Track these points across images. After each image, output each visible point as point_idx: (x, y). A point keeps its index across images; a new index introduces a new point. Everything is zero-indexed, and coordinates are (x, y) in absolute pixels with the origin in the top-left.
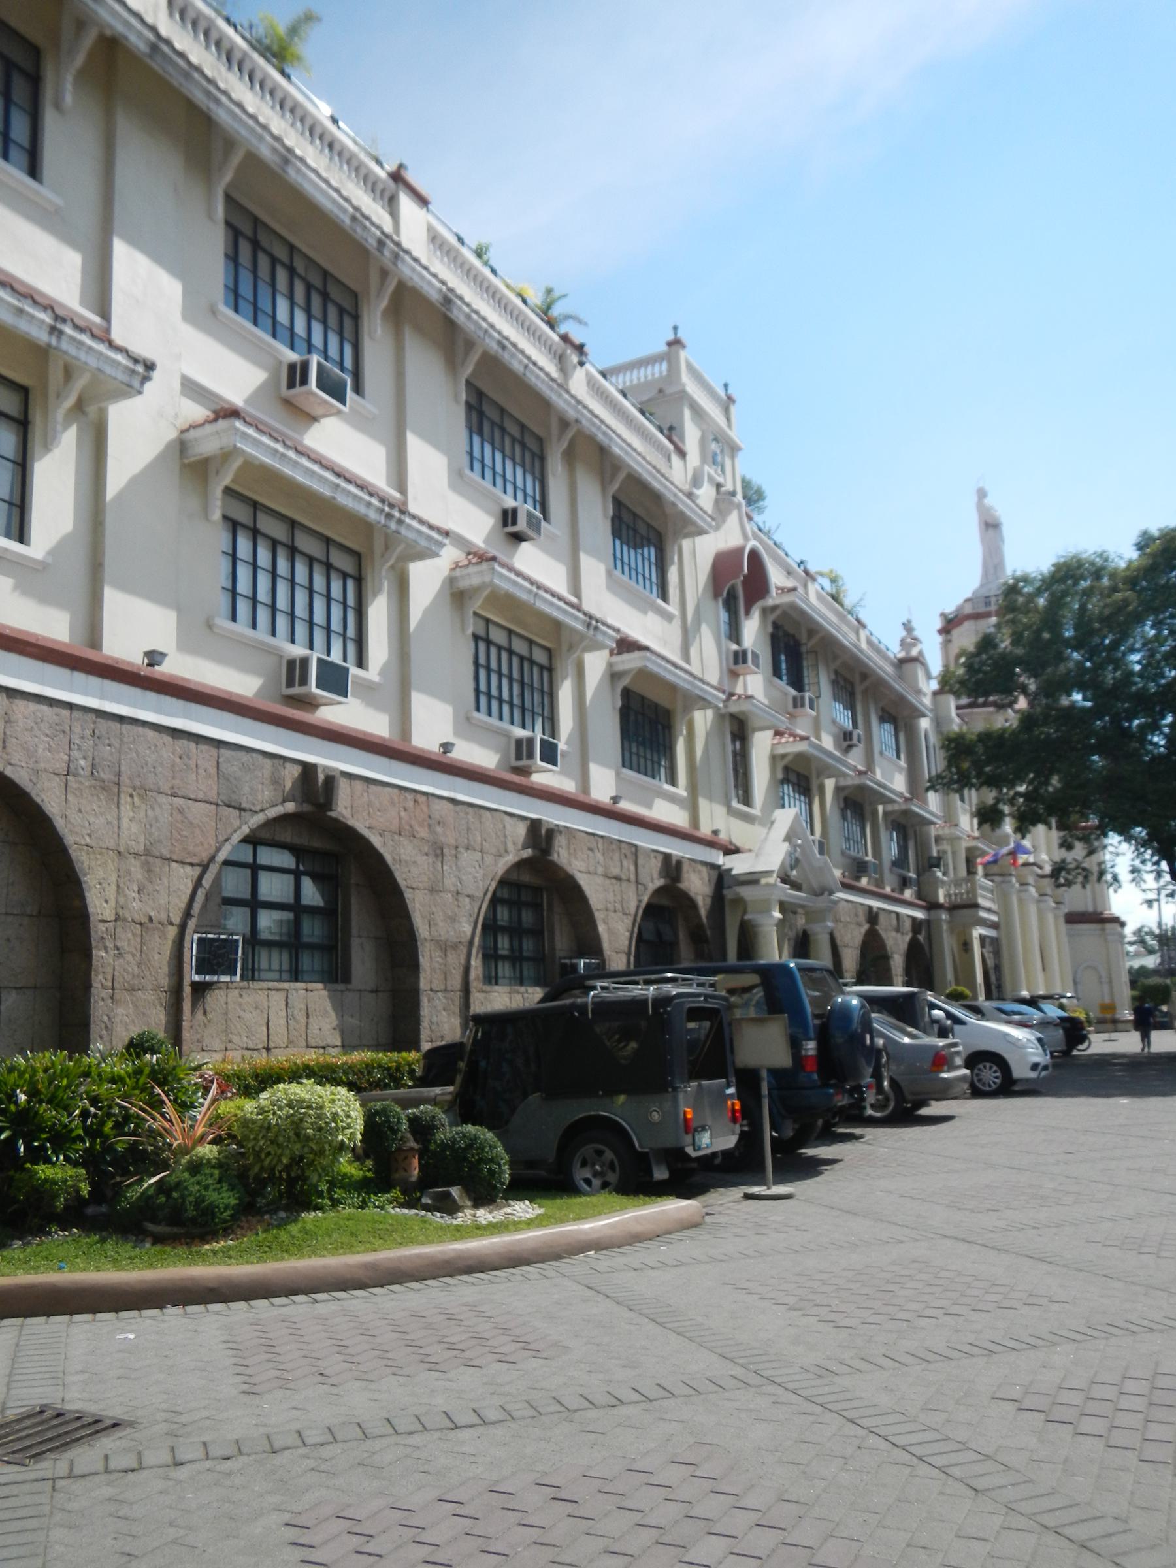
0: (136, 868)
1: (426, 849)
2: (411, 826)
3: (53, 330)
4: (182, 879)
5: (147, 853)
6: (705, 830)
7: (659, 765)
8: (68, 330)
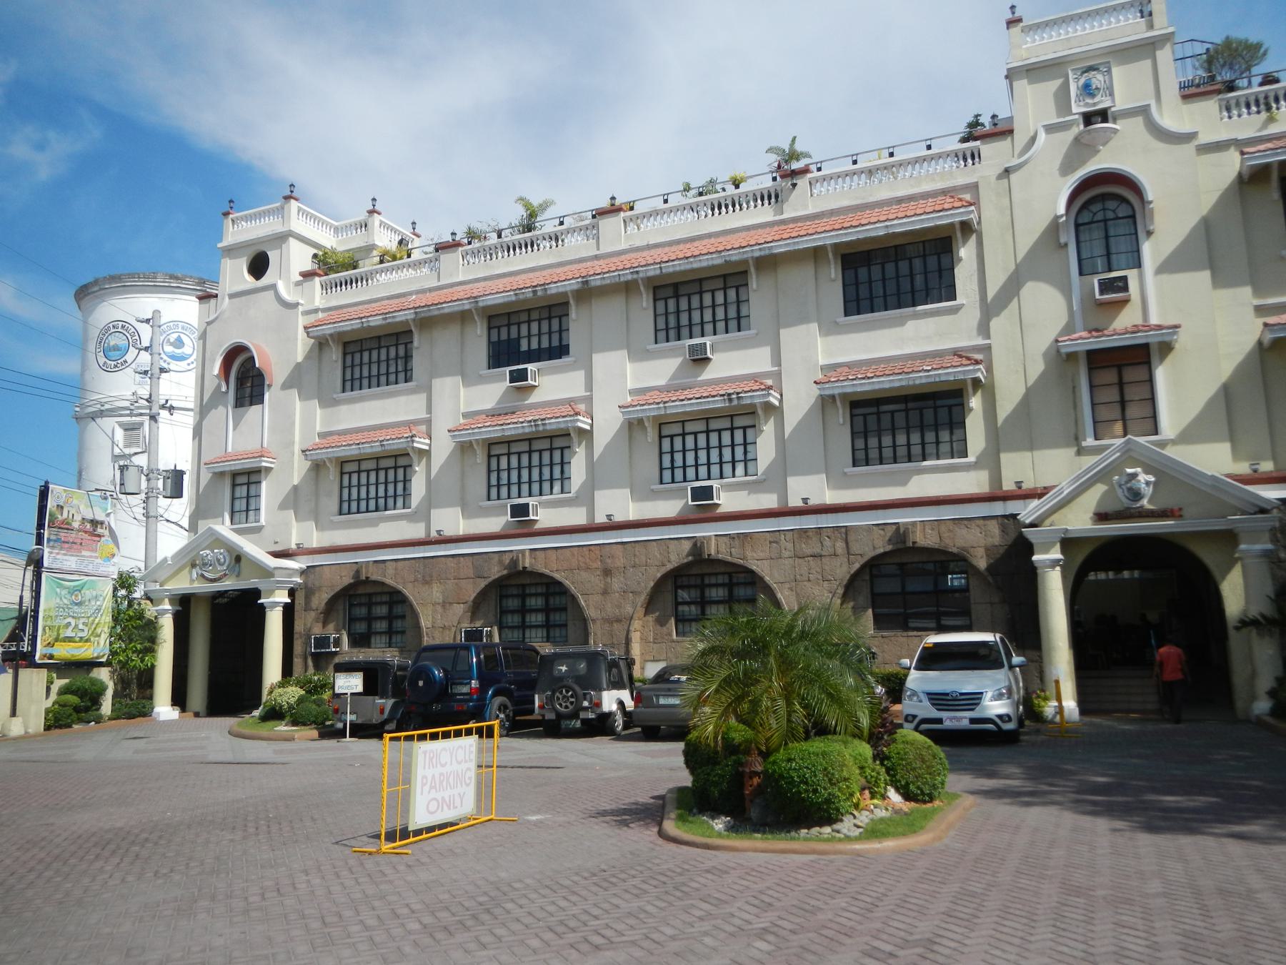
0: (439, 608)
1: (598, 573)
2: (586, 564)
3: (382, 445)
4: (459, 609)
5: (444, 602)
6: (1008, 486)
7: (938, 443)
8: (385, 443)
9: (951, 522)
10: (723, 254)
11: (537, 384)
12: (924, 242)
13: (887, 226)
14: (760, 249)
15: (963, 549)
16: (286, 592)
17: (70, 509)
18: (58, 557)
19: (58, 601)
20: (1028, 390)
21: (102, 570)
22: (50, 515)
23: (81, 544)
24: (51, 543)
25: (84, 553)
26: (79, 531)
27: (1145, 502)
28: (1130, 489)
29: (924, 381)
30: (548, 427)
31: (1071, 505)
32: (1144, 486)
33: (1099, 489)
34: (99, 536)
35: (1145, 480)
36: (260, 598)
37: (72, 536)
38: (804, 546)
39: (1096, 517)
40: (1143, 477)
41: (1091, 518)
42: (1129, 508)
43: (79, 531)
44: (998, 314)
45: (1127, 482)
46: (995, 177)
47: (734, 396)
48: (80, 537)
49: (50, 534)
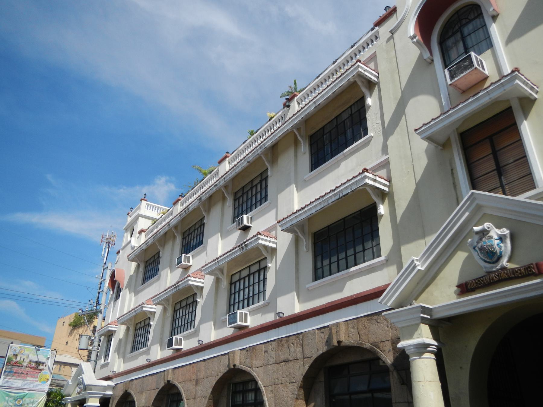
9: (366, 319)
10: (246, 158)
11: (191, 264)
12: (351, 107)
13: (315, 103)
14: (260, 148)
15: (375, 344)
16: (98, 400)
17: (22, 356)
18: (10, 380)
19: (6, 403)
20: (417, 185)
21: (40, 387)
22: (8, 359)
23: (27, 374)
24: (6, 373)
25: (28, 378)
26: (27, 367)
27: (504, 262)
28: (482, 249)
29: (333, 199)
30: (180, 287)
31: (436, 281)
32: (496, 242)
33: (461, 257)
34: (41, 370)
35: (498, 235)
36: (85, 403)
37: (22, 370)
38: (280, 353)
39: (460, 290)
40: (495, 233)
41: (455, 293)
42: (489, 273)
43: (27, 367)
44: (392, 133)
45: (478, 243)
46: (385, 42)
47: (243, 245)
48: (26, 370)
49: (6, 369)
